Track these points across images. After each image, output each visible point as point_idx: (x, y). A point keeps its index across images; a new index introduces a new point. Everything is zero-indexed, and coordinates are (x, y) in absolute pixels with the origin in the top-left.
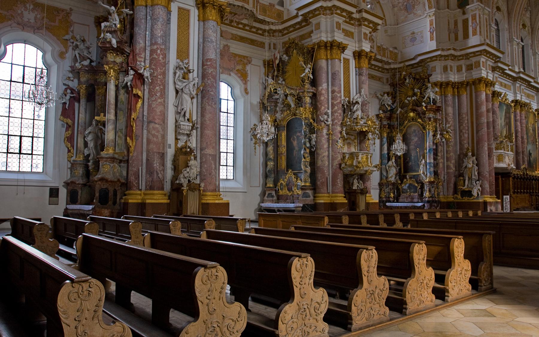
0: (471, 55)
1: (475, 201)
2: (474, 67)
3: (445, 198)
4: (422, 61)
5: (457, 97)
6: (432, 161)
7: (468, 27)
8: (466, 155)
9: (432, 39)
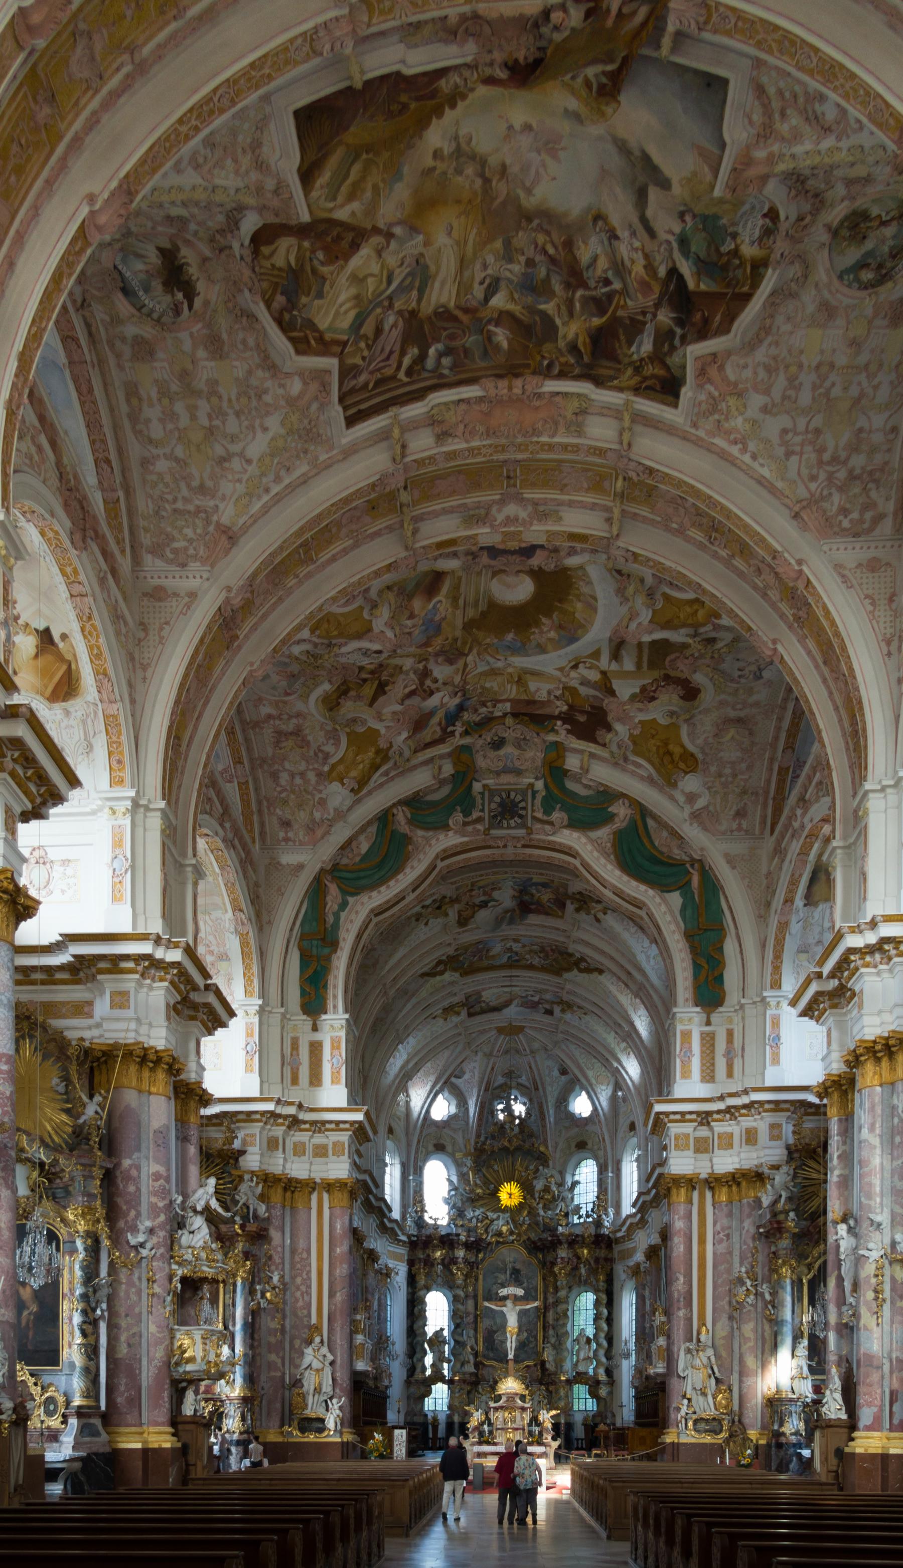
4: (225, 1114)
9: (248, 1069)
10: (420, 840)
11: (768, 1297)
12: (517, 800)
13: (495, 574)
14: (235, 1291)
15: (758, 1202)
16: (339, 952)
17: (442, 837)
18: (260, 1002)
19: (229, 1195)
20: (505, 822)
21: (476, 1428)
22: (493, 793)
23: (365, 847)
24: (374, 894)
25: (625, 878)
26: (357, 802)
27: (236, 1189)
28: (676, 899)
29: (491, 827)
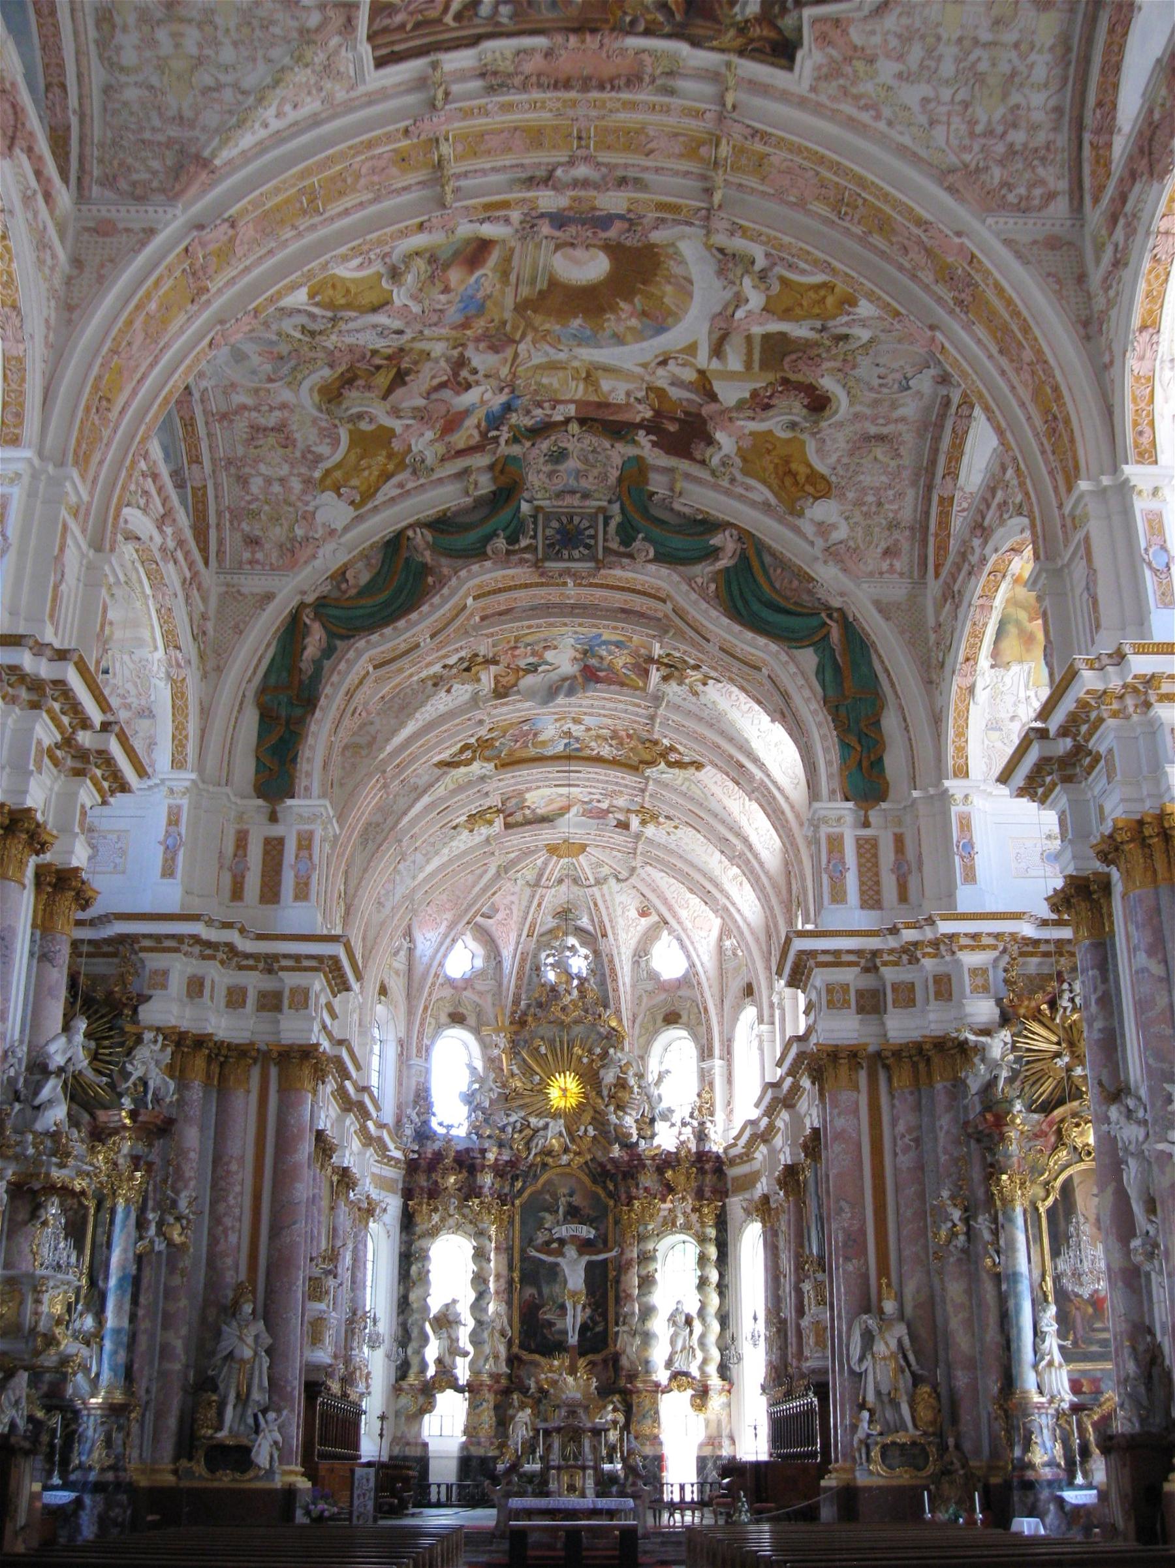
0: (284, 963)
1: (259, 1485)
2: (286, 1003)
3: (143, 1472)
4: (123, 939)
5: (215, 1095)
6: (125, 1324)
7: (280, 864)
8: (232, 1310)
10: (445, 571)
11: (987, 1236)
12: (582, 526)
13: (558, 247)
14: (112, 1222)
15: (959, 1085)
16: (318, 714)
17: (475, 568)
18: (193, 776)
19: (116, 1064)
20: (566, 552)
21: (514, 1467)
22: (548, 517)
23: (365, 578)
24: (375, 637)
25: (737, 628)
26: (359, 519)
27: (129, 1053)
28: (809, 658)
29: (546, 558)
